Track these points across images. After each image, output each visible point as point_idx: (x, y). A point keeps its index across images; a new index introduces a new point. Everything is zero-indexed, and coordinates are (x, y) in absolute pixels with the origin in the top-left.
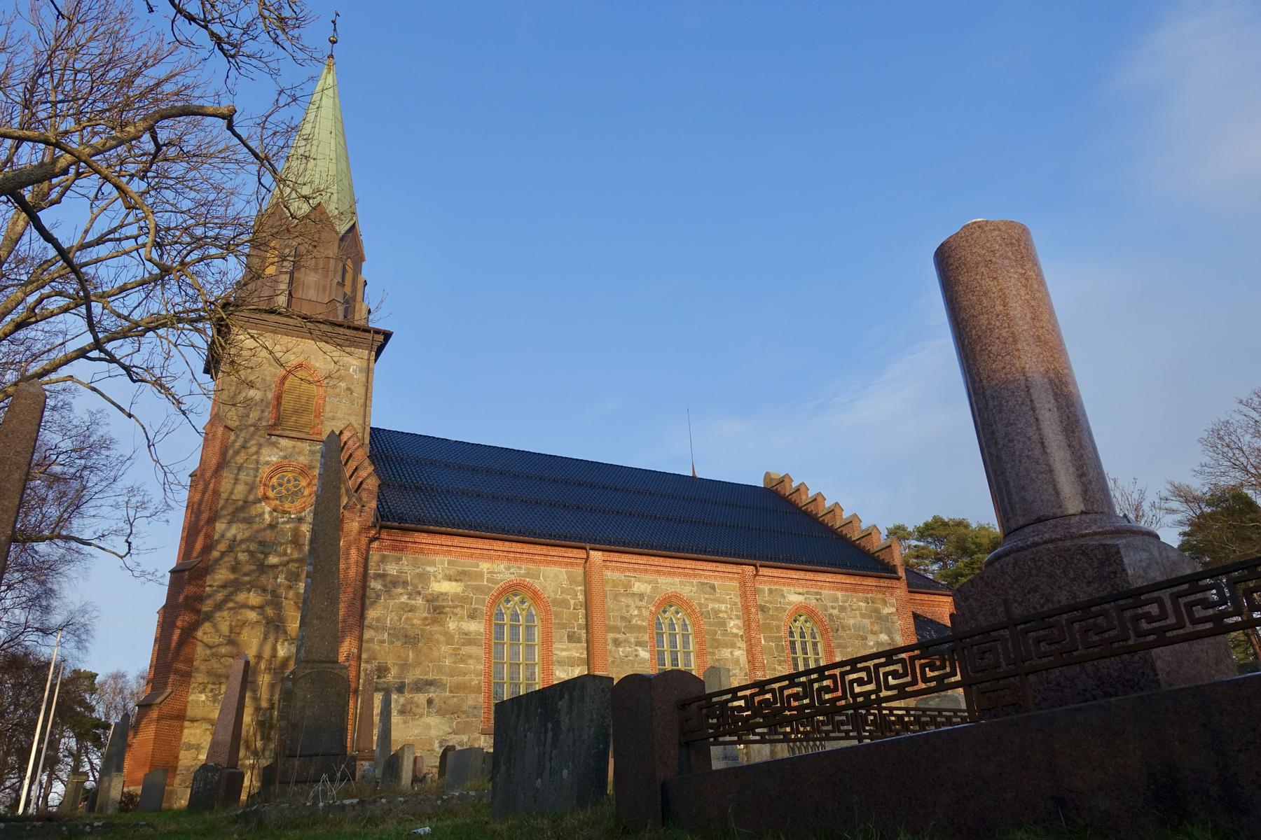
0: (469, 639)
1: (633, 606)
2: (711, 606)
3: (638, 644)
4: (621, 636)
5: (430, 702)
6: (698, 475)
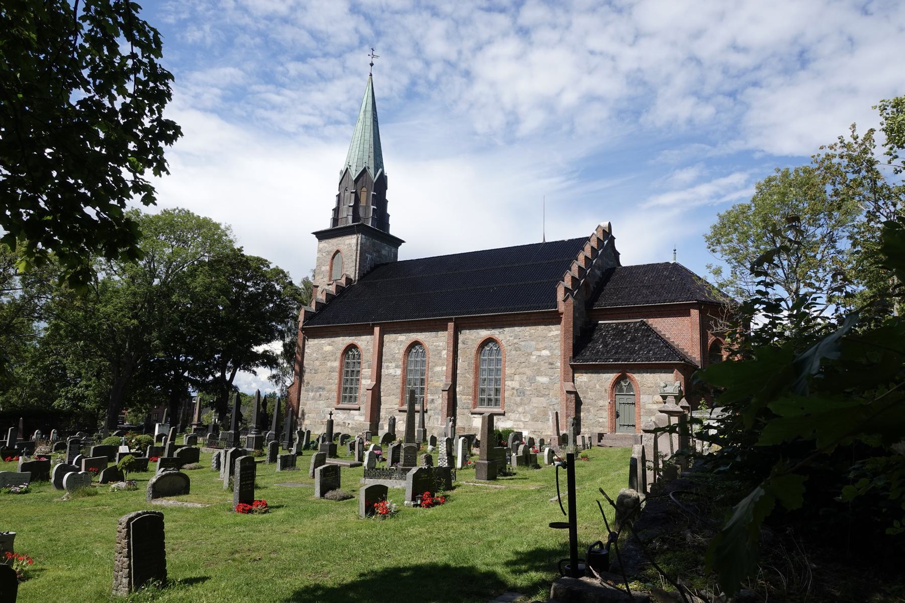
0: (332, 370)
1: (396, 348)
2: (435, 344)
3: (397, 367)
4: (390, 365)
5: (320, 395)
6: (547, 241)
